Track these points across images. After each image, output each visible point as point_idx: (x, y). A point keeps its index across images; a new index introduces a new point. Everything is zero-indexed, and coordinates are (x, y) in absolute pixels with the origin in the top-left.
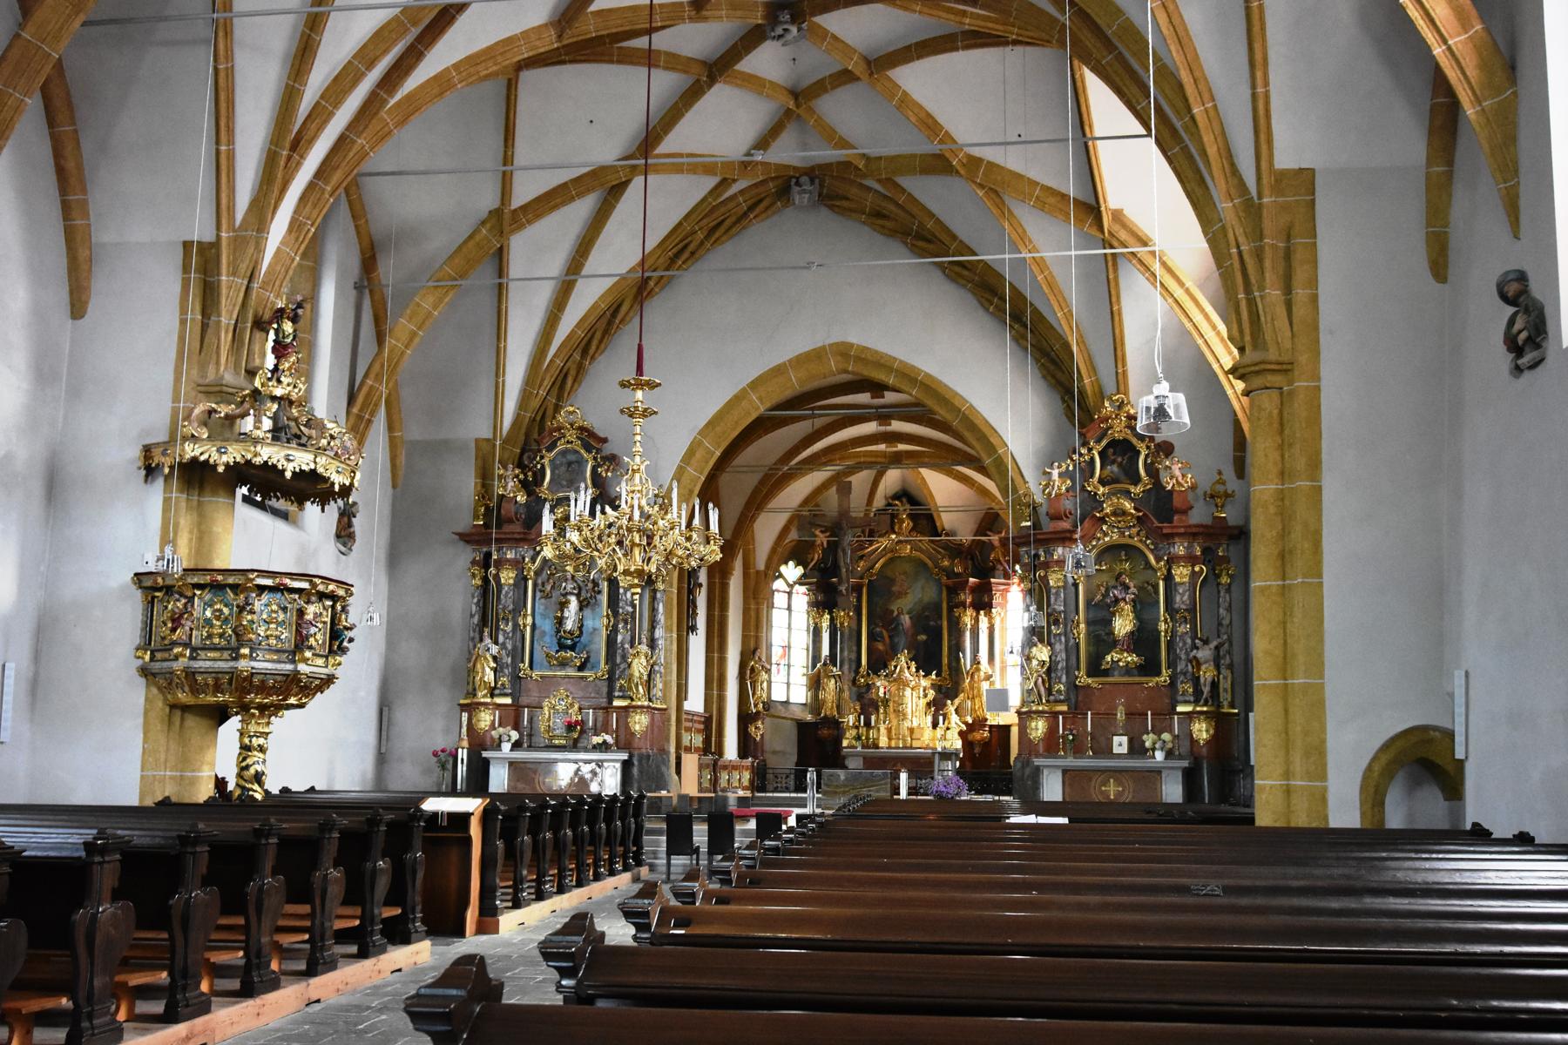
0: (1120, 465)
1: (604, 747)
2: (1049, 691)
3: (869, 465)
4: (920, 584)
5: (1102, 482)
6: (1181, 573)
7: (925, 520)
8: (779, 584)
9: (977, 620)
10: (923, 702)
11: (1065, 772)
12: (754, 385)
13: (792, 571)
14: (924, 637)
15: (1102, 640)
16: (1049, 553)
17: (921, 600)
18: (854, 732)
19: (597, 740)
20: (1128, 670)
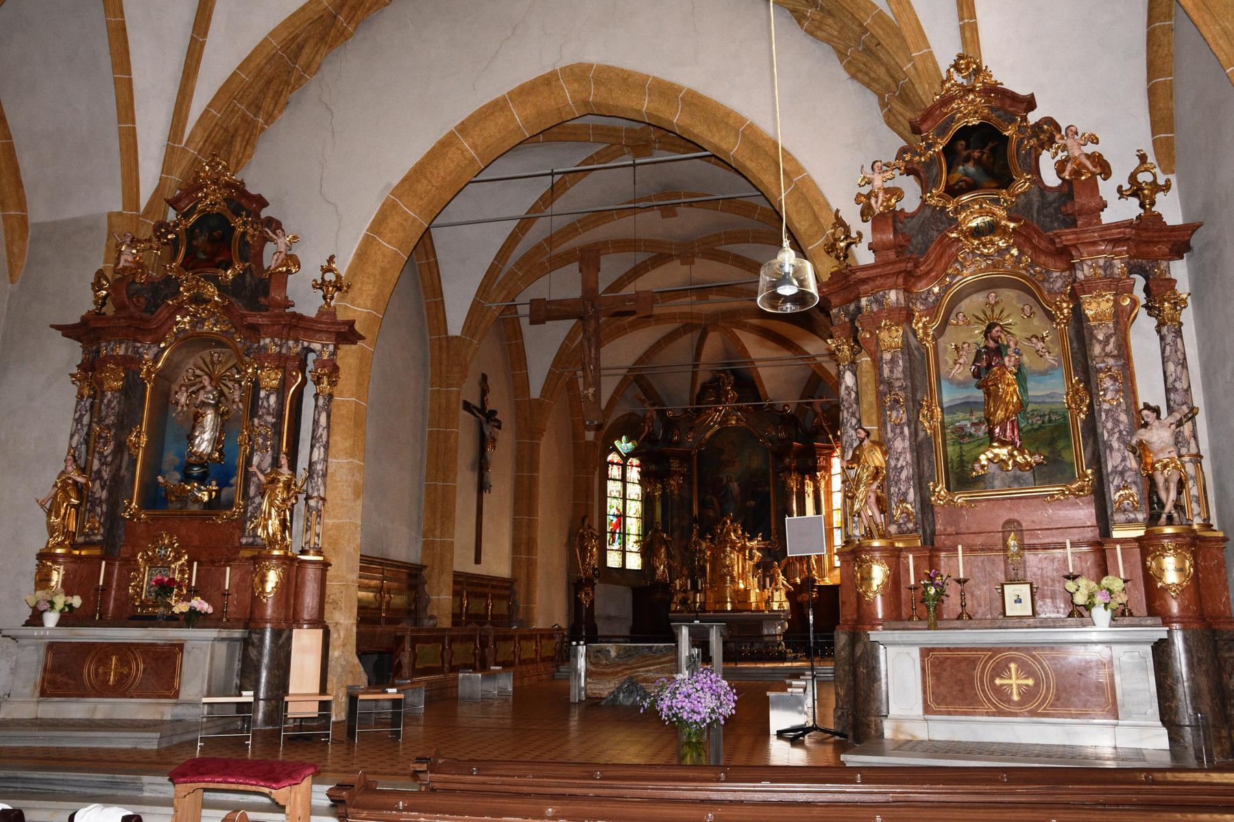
0: (978, 163)
1: (193, 619)
3: (687, 328)
7: (747, 384)
8: (613, 457)
9: (803, 485)
10: (749, 564)
12: (463, 128)
13: (624, 445)
14: (753, 503)
18: (680, 596)
19: (181, 608)
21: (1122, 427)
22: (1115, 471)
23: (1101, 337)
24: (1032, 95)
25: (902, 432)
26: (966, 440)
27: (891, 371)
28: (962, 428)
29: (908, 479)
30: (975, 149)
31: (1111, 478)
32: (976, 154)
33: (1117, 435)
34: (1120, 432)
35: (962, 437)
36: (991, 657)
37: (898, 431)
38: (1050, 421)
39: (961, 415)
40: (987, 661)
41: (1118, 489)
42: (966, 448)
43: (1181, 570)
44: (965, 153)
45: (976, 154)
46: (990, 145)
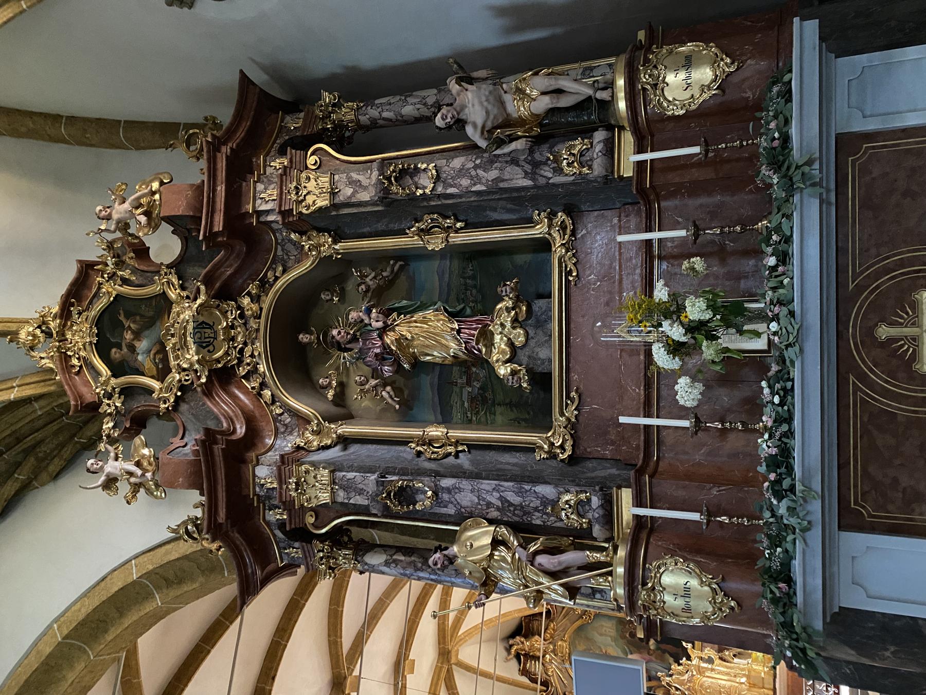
0: (137, 335)
2: (580, 538)
4: (599, 639)
5: (162, 373)
6: (315, 193)
11: (850, 519)
15: (461, 386)
16: (266, 500)
17: (614, 640)
20: (532, 321)
21: (470, 165)
22: (532, 175)
23: (349, 191)
24: (80, 261)
25: (448, 490)
26: (489, 395)
27: (360, 492)
28: (472, 400)
29: (520, 492)
30: (122, 336)
31: (542, 181)
32: (128, 336)
33: (480, 172)
34: (476, 167)
35: (484, 401)
36: (863, 377)
37: (446, 496)
38: (473, 278)
39: (455, 398)
40: (871, 385)
41: (559, 171)
42: (500, 397)
43: (688, 63)
44: (125, 350)
45: (128, 336)
46: (122, 318)
